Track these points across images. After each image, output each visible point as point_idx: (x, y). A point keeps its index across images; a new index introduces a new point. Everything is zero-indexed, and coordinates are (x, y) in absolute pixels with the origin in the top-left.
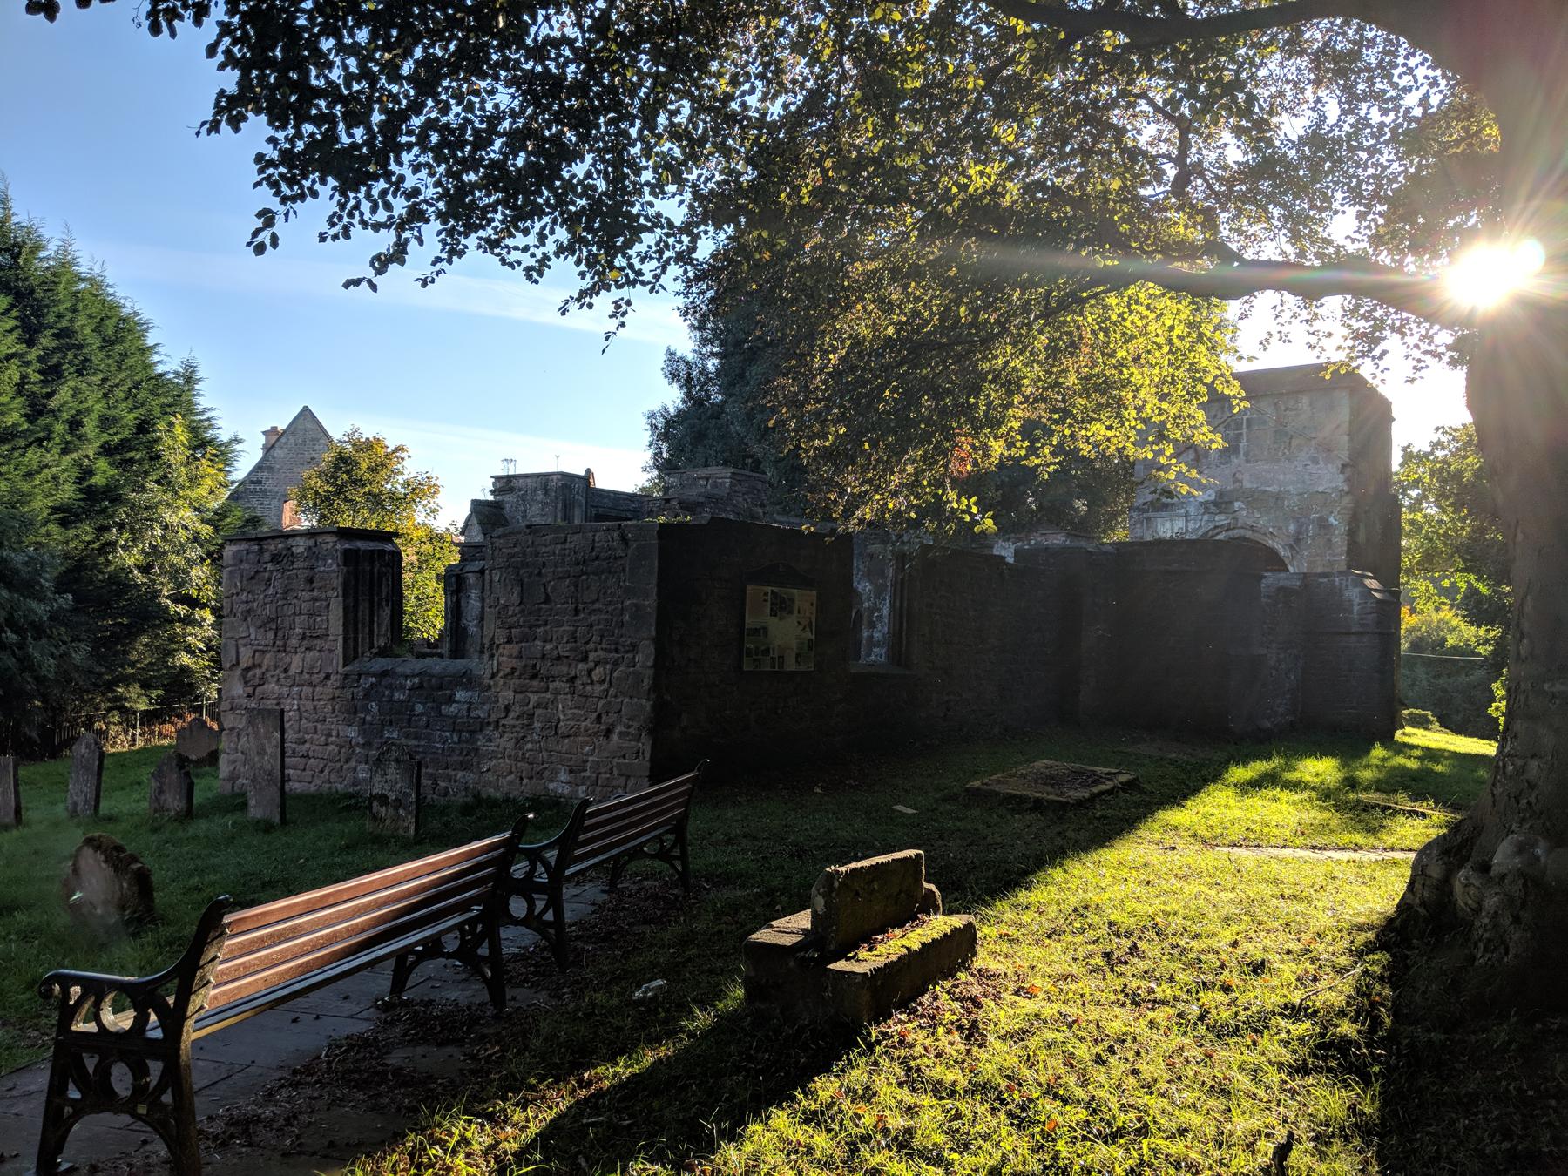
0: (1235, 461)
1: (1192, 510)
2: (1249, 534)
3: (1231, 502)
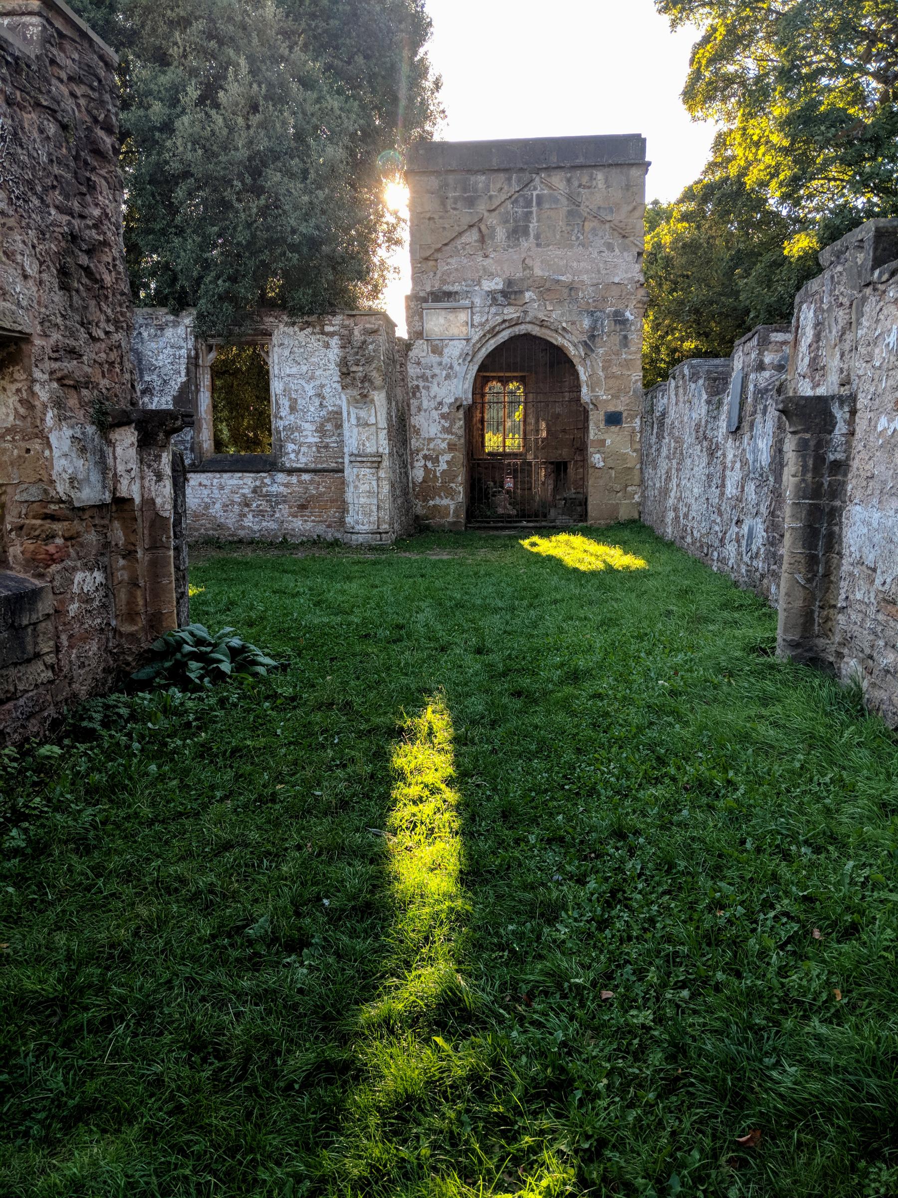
1: (478, 301)
2: (536, 331)
3: (521, 292)
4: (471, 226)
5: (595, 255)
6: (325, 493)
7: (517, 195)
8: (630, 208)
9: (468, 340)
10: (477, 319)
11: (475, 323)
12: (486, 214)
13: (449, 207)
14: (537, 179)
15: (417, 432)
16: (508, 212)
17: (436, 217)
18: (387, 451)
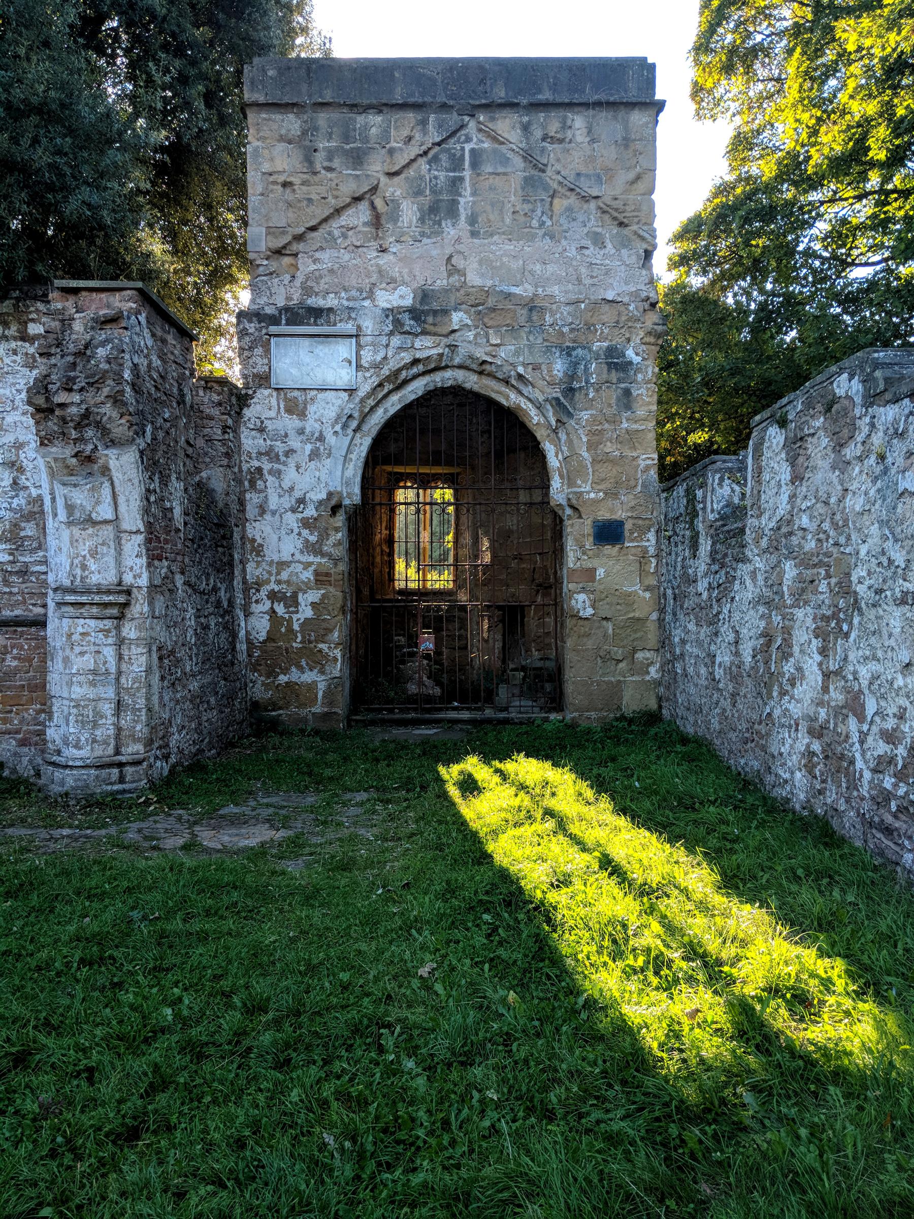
0: (450, 231)
1: (368, 325)
2: (471, 381)
3: (445, 312)
4: (357, 199)
5: (572, 252)
6: (17, 670)
7: (437, 149)
8: (631, 175)
9: (351, 391)
10: (367, 356)
11: (364, 363)
12: (384, 180)
13: (318, 167)
14: (472, 124)
15: (258, 550)
16: (421, 178)
17: (296, 180)
18: (144, 581)
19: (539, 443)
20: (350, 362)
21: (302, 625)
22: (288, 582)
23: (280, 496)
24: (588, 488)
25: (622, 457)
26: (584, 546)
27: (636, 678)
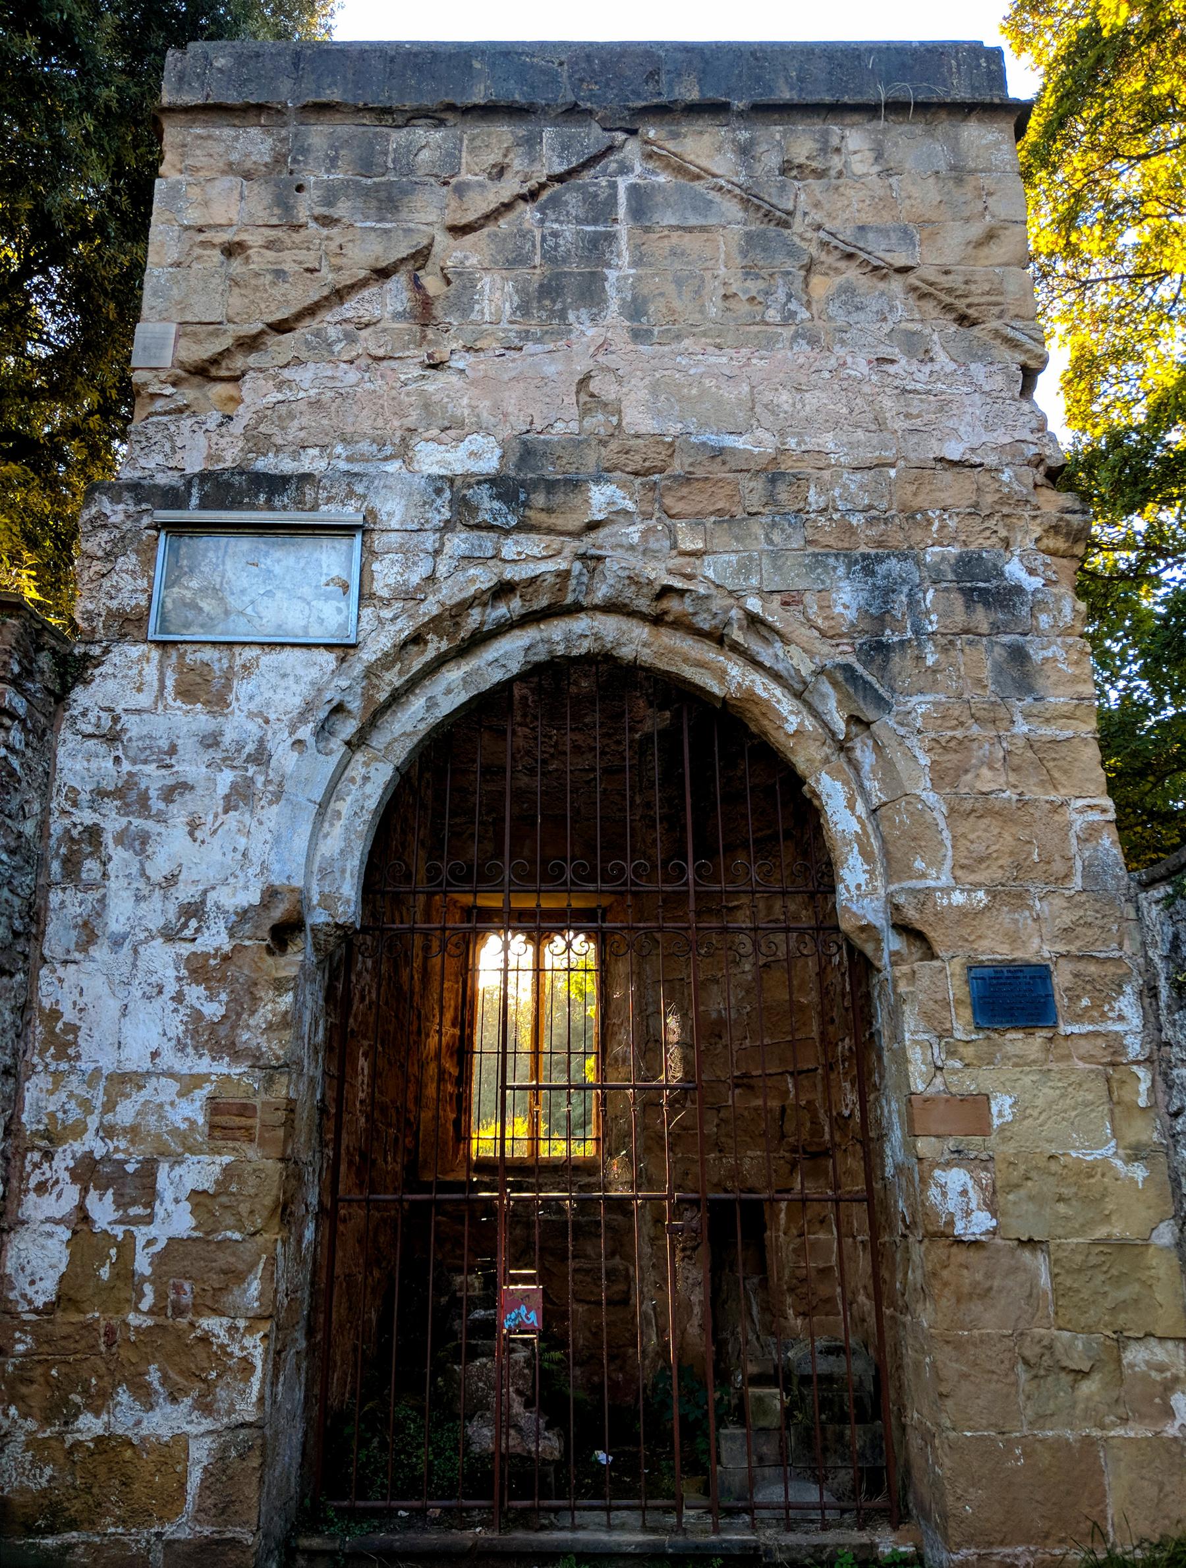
3: (575, 485)
4: (383, 273)
5: (860, 366)
8: (976, 230)
9: (344, 649)
11: (380, 587)
12: (442, 240)
13: (303, 215)
14: (632, 149)
16: (524, 234)
17: (254, 238)
19: (801, 781)
20: (345, 587)
21: (160, 1260)
22: (133, 1132)
23: (139, 899)
24: (945, 880)
25: (1023, 803)
26: (949, 1032)
27: (1135, 1431)
